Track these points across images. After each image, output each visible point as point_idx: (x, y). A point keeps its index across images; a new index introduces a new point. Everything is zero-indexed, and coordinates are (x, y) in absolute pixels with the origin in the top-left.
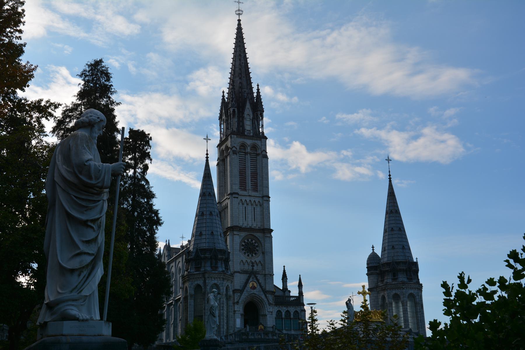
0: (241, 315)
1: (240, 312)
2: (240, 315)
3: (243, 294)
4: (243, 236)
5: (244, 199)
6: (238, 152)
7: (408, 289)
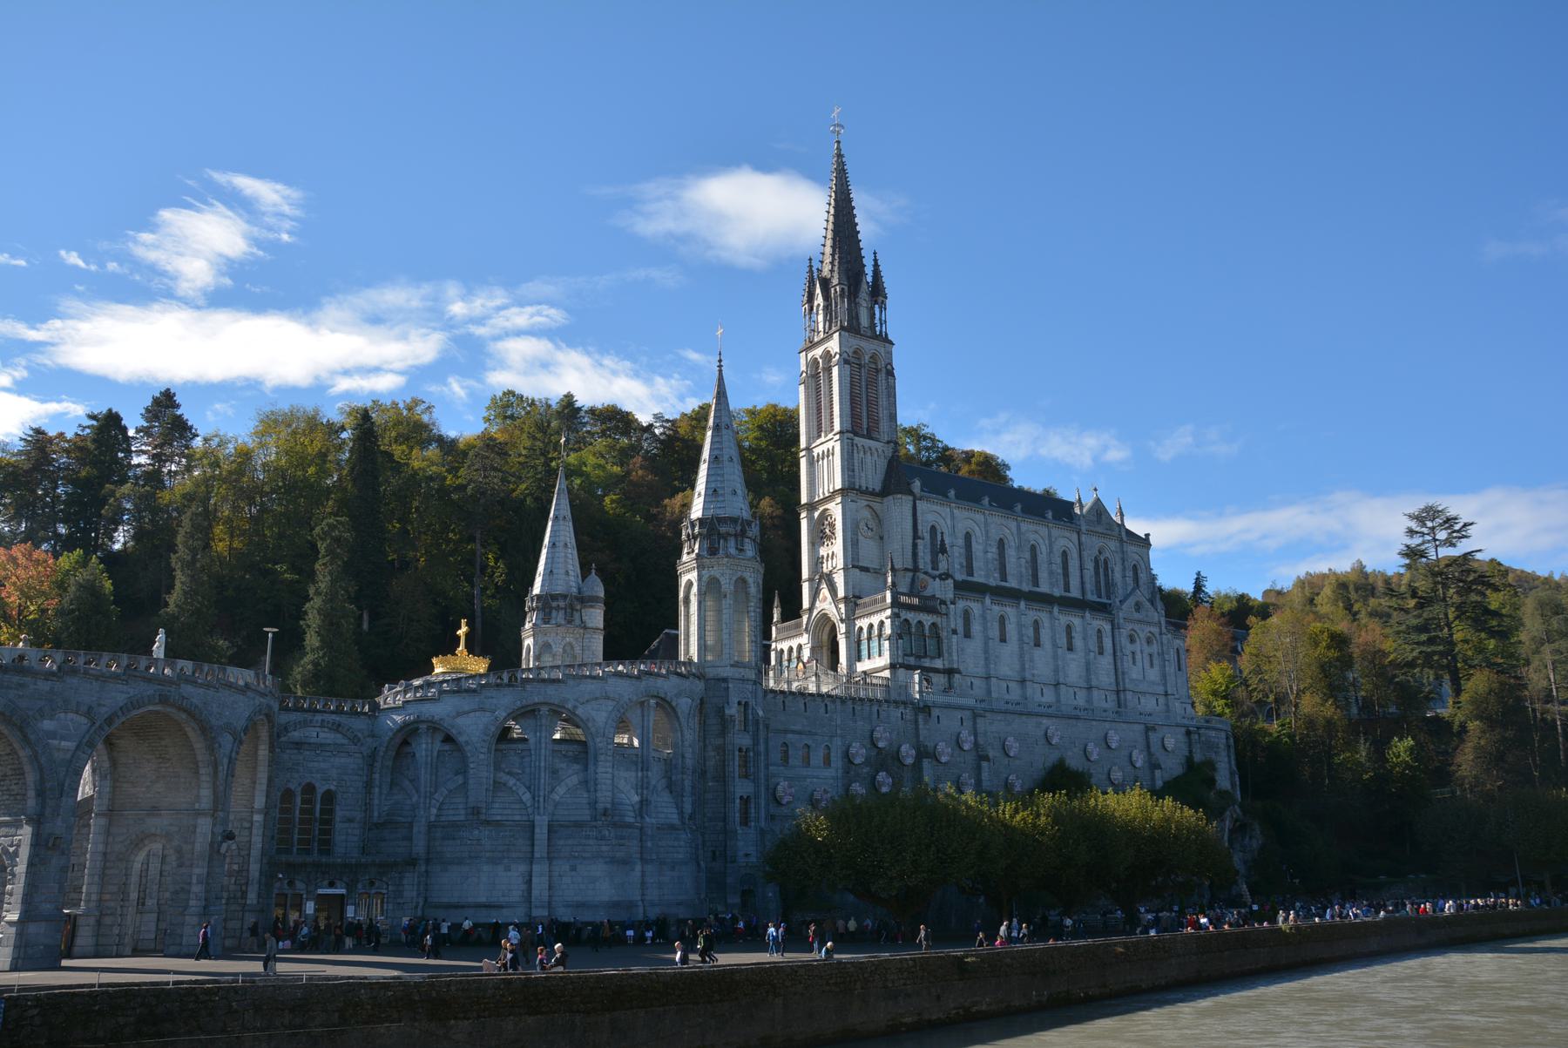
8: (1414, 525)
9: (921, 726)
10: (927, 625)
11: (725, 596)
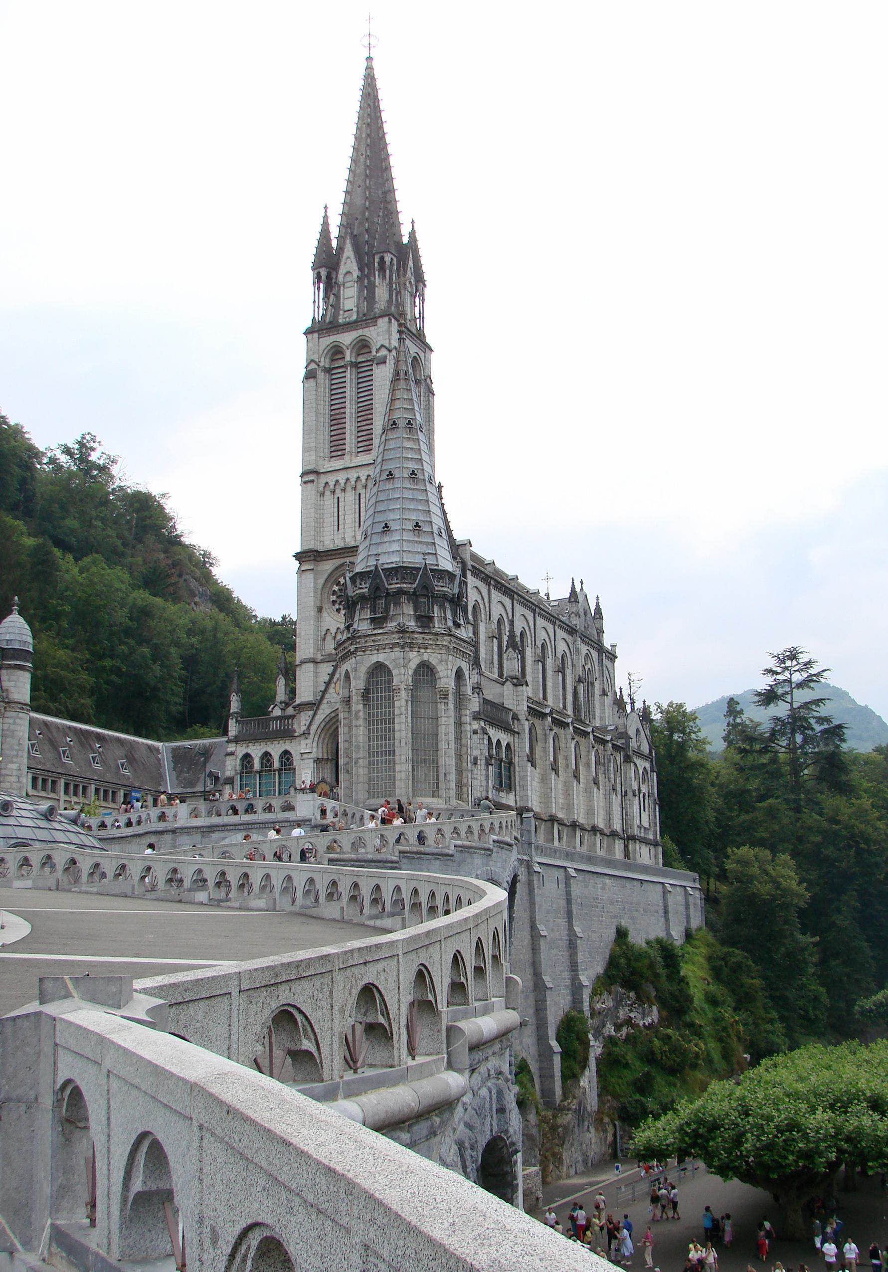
0: (318, 761)
1: (312, 756)
2: (312, 761)
3: (320, 712)
4: (329, 572)
5: (331, 479)
6: (328, 371)
7: (368, 652)
8: (772, 664)
9: (536, 891)
10: (504, 744)
11: (446, 696)
